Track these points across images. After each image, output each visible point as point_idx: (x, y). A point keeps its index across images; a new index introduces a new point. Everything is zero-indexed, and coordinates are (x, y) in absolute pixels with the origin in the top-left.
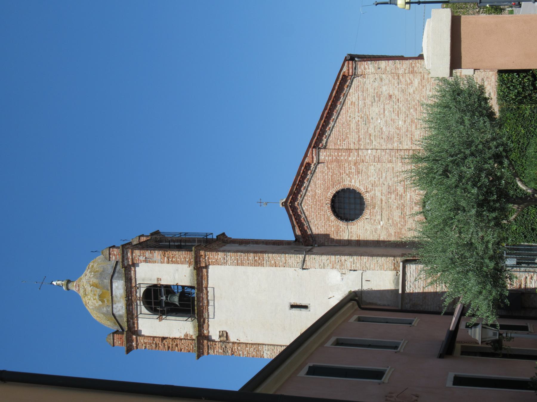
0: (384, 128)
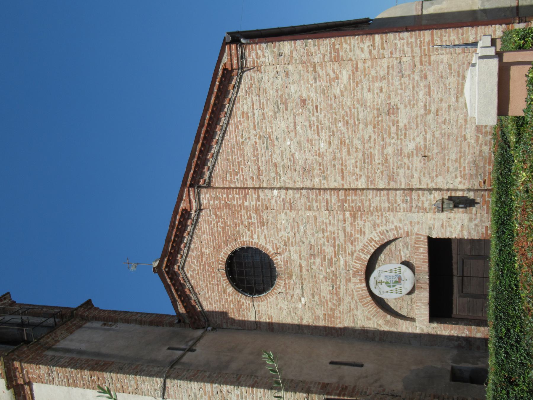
0: (297, 154)
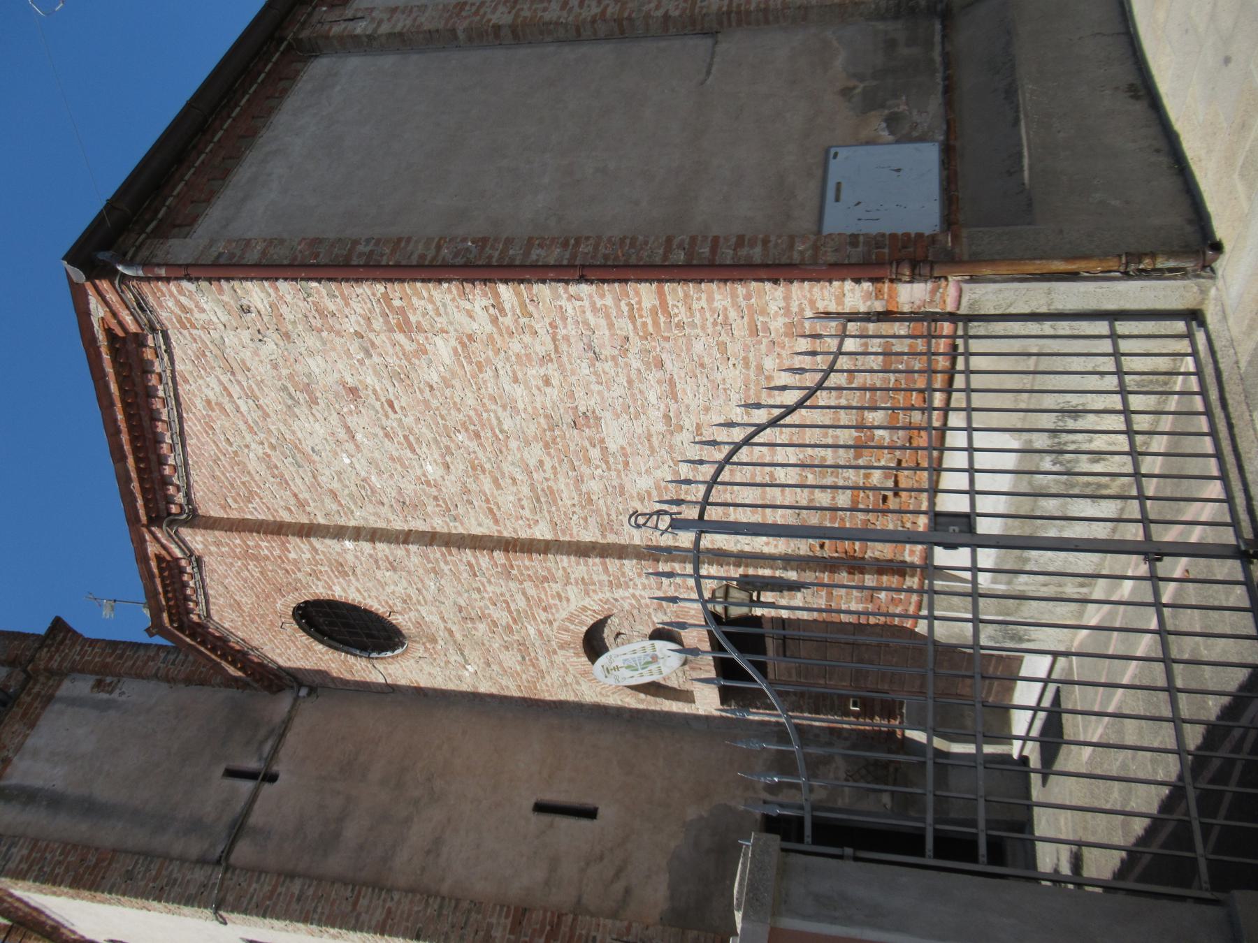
0: (373, 478)
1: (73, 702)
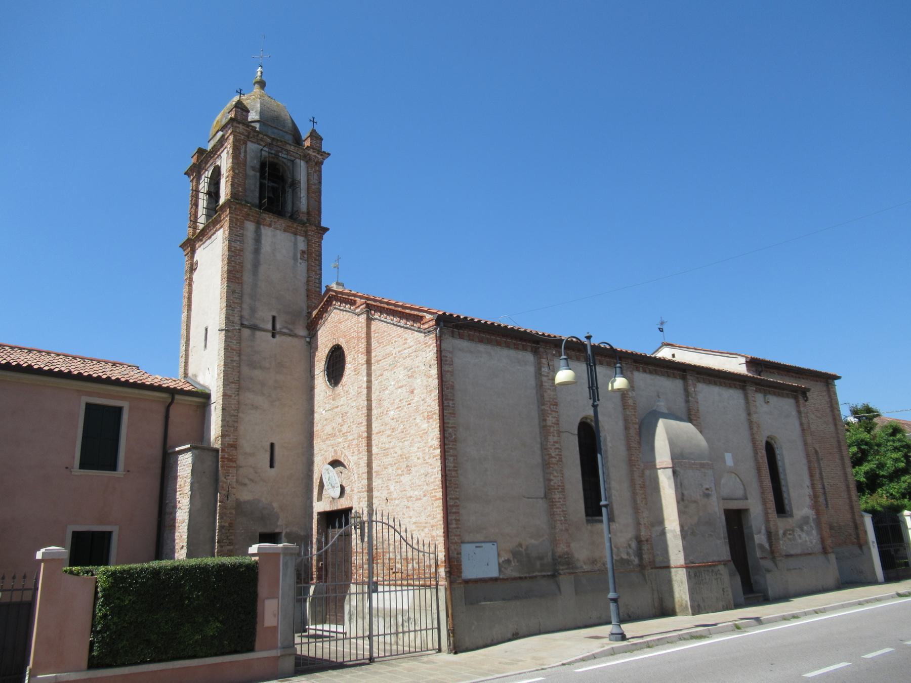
1: (295, 244)
